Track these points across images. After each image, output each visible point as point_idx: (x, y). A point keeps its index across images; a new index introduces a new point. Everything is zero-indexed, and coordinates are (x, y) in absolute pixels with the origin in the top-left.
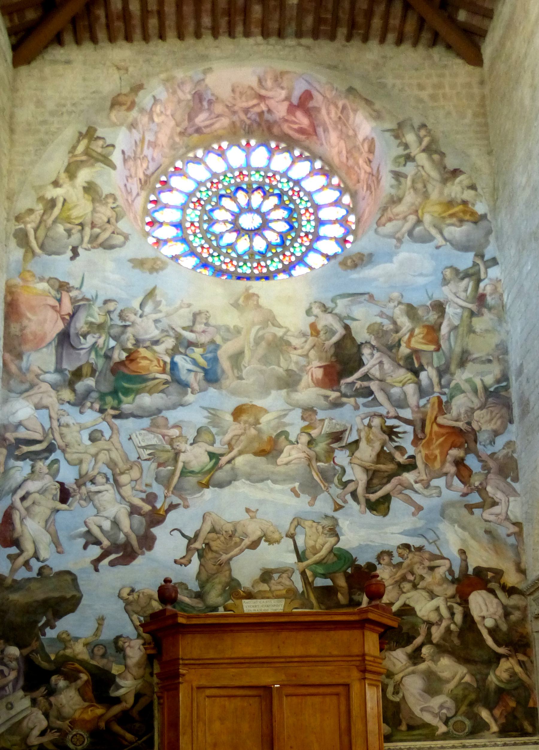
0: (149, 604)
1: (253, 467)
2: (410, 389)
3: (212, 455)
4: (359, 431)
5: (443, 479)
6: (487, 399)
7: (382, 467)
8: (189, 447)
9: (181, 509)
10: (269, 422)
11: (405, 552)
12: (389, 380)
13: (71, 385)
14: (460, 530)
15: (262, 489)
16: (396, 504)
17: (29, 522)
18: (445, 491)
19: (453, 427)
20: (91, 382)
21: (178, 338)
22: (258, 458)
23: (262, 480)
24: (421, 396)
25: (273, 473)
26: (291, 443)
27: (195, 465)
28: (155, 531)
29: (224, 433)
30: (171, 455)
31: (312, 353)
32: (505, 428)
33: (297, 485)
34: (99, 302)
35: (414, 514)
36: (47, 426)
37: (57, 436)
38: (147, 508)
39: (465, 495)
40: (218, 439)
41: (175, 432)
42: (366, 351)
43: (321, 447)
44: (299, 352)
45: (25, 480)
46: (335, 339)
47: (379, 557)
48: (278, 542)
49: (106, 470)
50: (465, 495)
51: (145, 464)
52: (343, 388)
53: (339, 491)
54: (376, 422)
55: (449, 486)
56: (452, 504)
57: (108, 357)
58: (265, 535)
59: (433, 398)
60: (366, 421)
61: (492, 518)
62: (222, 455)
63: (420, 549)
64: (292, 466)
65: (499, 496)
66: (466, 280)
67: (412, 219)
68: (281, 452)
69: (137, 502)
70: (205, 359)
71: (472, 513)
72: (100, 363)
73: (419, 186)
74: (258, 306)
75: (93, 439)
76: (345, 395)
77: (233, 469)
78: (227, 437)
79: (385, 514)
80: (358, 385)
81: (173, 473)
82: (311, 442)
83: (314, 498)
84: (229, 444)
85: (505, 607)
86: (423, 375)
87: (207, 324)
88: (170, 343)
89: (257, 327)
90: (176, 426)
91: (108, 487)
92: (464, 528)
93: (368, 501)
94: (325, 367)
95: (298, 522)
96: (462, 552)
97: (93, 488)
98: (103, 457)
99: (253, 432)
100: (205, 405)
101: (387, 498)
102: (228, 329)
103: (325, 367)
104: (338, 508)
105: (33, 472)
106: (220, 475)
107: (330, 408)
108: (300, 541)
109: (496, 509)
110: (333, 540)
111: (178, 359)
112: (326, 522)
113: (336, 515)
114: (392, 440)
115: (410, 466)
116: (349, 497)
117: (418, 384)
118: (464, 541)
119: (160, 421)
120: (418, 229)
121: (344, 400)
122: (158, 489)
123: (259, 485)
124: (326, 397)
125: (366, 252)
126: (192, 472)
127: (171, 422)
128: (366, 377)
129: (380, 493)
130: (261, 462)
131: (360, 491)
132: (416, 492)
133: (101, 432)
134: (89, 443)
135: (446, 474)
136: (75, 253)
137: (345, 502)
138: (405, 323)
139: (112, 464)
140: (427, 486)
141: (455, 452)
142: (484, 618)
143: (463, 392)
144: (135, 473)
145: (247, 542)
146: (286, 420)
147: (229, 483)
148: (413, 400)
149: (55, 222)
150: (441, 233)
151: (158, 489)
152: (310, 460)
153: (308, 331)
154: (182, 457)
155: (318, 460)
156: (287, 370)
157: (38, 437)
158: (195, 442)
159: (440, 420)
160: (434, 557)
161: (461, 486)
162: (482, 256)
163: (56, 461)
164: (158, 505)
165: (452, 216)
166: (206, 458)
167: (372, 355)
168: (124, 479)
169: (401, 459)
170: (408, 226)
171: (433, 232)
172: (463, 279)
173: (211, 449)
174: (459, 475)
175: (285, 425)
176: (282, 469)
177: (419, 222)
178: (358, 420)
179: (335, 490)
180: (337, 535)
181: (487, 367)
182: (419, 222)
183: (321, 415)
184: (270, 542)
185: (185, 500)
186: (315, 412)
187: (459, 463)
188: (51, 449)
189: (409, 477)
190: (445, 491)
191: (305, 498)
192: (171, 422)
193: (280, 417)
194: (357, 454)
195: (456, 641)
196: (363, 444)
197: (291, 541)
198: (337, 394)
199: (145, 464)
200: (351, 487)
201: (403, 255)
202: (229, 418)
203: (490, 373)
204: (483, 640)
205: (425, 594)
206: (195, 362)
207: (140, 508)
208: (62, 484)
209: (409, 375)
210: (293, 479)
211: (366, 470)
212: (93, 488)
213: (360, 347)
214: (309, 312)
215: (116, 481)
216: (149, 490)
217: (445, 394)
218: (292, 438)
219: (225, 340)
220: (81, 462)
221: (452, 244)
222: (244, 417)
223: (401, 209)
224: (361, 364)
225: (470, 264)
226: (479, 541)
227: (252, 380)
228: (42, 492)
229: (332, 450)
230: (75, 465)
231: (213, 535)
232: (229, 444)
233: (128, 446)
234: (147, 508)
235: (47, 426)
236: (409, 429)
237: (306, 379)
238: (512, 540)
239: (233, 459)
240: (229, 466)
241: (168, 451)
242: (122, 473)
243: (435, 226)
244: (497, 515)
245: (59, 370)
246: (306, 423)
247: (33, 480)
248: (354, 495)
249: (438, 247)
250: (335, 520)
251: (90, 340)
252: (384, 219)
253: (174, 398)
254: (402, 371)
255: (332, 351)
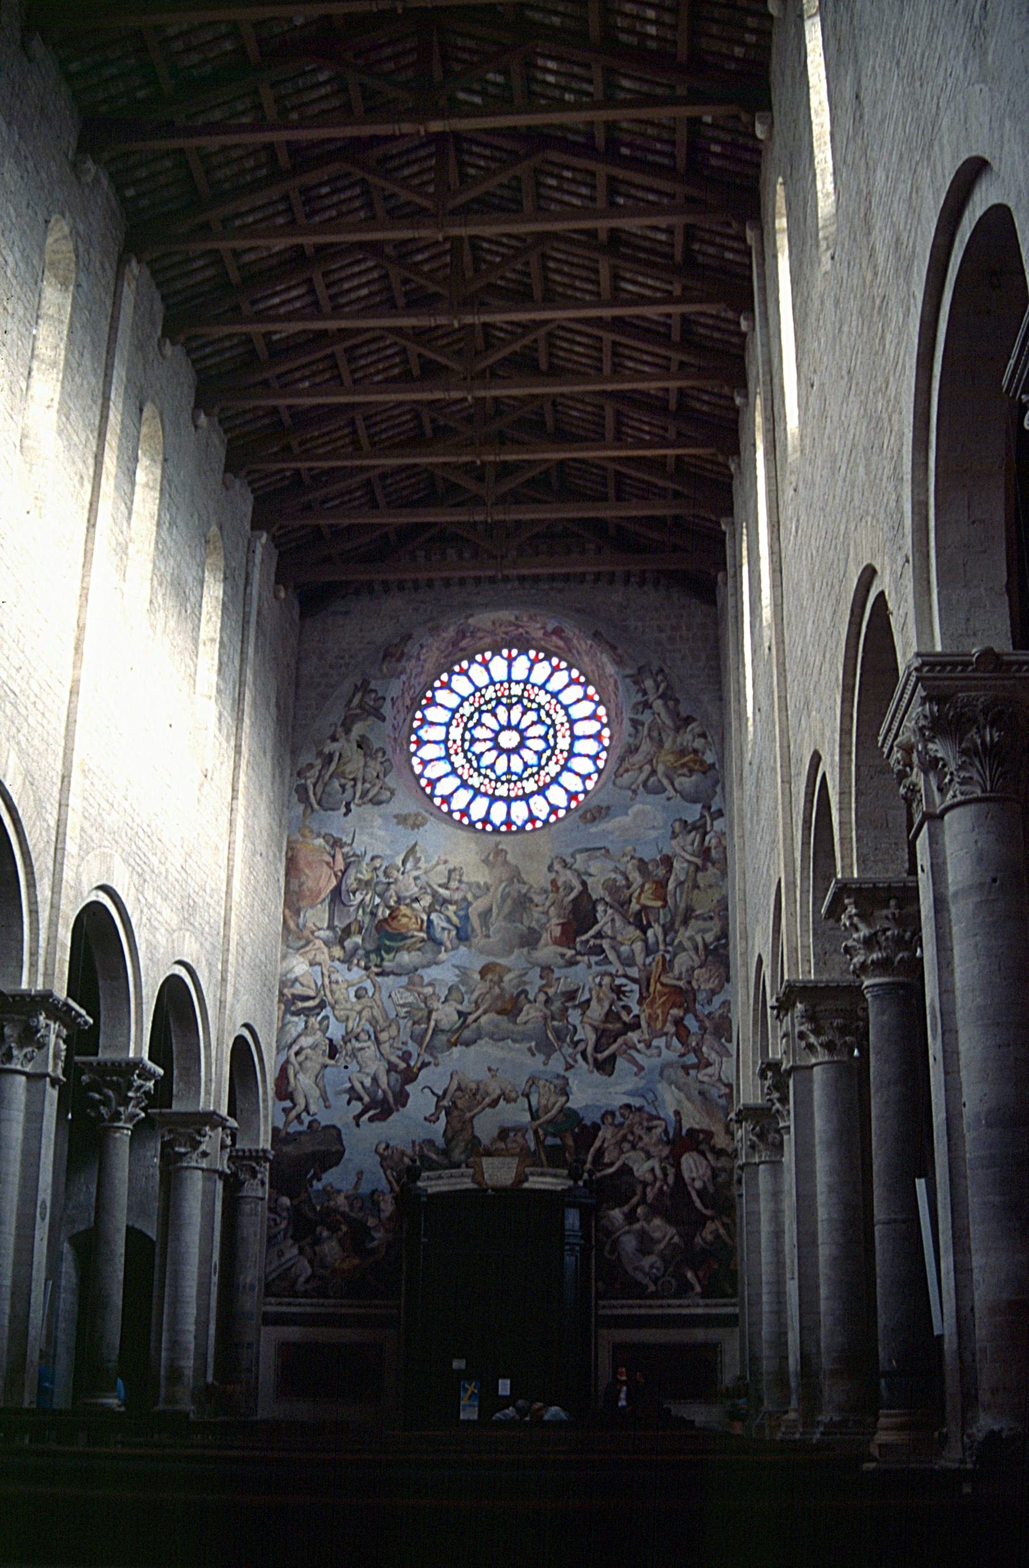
0: (401, 1160)
1: (497, 1026)
2: (638, 946)
3: (460, 1014)
4: (590, 990)
5: (664, 1039)
6: (707, 957)
7: (610, 1026)
8: (440, 1006)
9: (432, 1067)
10: (511, 980)
11: (626, 1113)
12: (619, 938)
13: (341, 942)
14: (676, 1091)
15: (502, 1048)
16: (621, 1063)
17: (301, 1076)
18: (664, 1051)
19: (675, 986)
20: (358, 939)
21: (435, 894)
22: (500, 1017)
23: (503, 1039)
24: (647, 955)
25: (513, 1032)
26: (530, 1002)
27: (445, 1025)
28: (408, 1088)
29: (472, 992)
30: (425, 1013)
31: (552, 911)
32: (722, 987)
33: (533, 1044)
34: (368, 858)
35: (636, 1074)
36: (319, 983)
37: (328, 994)
38: (403, 1065)
39: (682, 1055)
40: (466, 997)
41: (429, 990)
42: (600, 908)
43: (556, 1006)
44: (540, 909)
45: (299, 1036)
46: (573, 895)
47: (603, 1117)
48: (515, 1100)
49: (368, 1027)
50: (682, 1055)
51: (401, 1021)
52: (578, 947)
53: (570, 1050)
54: (607, 980)
55: (668, 1047)
56: (669, 1065)
57: (373, 914)
58: (503, 1094)
59: (658, 957)
60: (598, 980)
61: (706, 1079)
62: (470, 1014)
63: (640, 1109)
64: (529, 1026)
65: (713, 1057)
66: (693, 834)
67: (647, 768)
68: (521, 1011)
69: (394, 1059)
70: (458, 916)
71: (688, 1074)
72: (367, 919)
73: (655, 734)
74: (506, 862)
75: (358, 997)
76: (578, 953)
77: (478, 1028)
78: (476, 994)
79: (610, 1075)
80: (591, 943)
81: (427, 1030)
82: (548, 1001)
83: (548, 1057)
84: (476, 1002)
85: (713, 1169)
86: (650, 933)
87: (460, 881)
88: (426, 901)
89: (503, 885)
90: (430, 984)
91: (369, 1043)
92: (679, 1089)
93: (595, 1060)
94: (563, 925)
95: (533, 1081)
96: (677, 1113)
97: (358, 1045)
98: (366, 1014)
99: (497, 990)
100: (458, 963)
101: (613, 1057)
102: (478, 885)
103: (563, 925)
104: (569, 1067)
105: (306, 1027)
106: (467, 1034)
107: (566, 966)
108: (534, 1101)
109: (710, 1070)
110: (563, 1099)
111: (433, 916)
112: (556, 1082)
113: (567, 1074)
114: (620, 999)
115: (635, 1026)
116: (579, 1057)
117: (645, 941)
118: (679, 1102)
119: (417, 979)
120: (652, 779)
121: (579, 958)
122: (412, 1047)
123: (500, 1044)
124: (563, 955)
125: (604, 804)
126: (443, 1031)
127: (426, 980)
128: (599, 935)
129: (606, 1053)
130: (503, 1021)
131: (590, 1050)
132: (638, 1051)
133: (366, 989)
134: (354, 1000)
135: (666, 1034)
136: (348, 810)
137: (576, 1061)
138: (636, 877)
139: (373, 1021)
140: (649, 1046)
141: (675, 1012)
142: (693, 1180)
143: (685, 950)
144: (393, 1031)
145: (488, 1100)
146: (526, 979)
147: (475, 1042)
148: (639, 959)
149: (331, 777)
150: (672, 784)
151: (412, 1047)
152: (545, 1018)
153: (549, 887)
154: (434, 1016)
155: (553, 1019)
156: (529, 928)
157: (312, 993)
158: (446, 1000)
159: (664, 979)
160: (652, 1118)
161: (679, 1045)
162: (709, 808)
163: (326, 1017)
164: (412, 1063)
165: (683, 765)
166: (456, 1017)
167: (606, 911)
168: (384, 1036)
169: (626, 1018)
170: (643, 776)
171: (665, 782)
172: (690, 832)
173: (460, 1007)
174: (677, 1034)
175: (525, 983)
176: (521, 1028)
177: (654, 772)
178: (590, 978)
179: (568, 1050)
180: (567, 1095)
181: (709, 924)
182: (654, 772)
183: (557, 973)
184: (508, 1101)
185: (436, 1058)
186: (553, 971)
187: (678, 1022)
188: (322, 1005)
189: (633, 1036)
190: (664, 1051)
191: (540, 1057)
192: (426, 980)
193: (521, 976)
194: (588, 1013)
195: (668, 1202)
196: (594, 1003)
197: (526, 1100)
198: (573, 952)
199: (401, 1021)
200: (581, 1047)
201: (637, 807)
202: (477, 977)
203: (711, 930)
204: (693, 1203)
205: (643, 1155)
206: (449, 920)
207: (396, 1066)
208: (331, 1041)
209: (638, 933)
210: (530, 1039)
211: (595, 1029)
212: (358, 1045)
213: (595, 903)
214: (550, 868)
215: (376, 1038)
216: (404, 1048)
217: (668, 952)
218: (531, 997)
219: (476, 897)
220: (347, 1019)
221: (682, 797)
222: (489, 976)
223: (638, 758)
224: (596, 922)
225: (698, 816)
226: (693, 1102)
227: (498, 937)
228: (314, 1047)
229: (566, 1009)
230: (342, 1022)
231: (459, 1093)
232: (476, 1002)
233: (388, 1005)
234: (403, 1065)
235: (319, 983)
236: (636, 987)
237: (546, 937)
238: (723, 1102)
239: (479, 1017)
240: (474, 1025)
241: (421, 1009)
242: (382, 1031)
243: (668, 777)
244: (710, 1076)
245: (331, 927)
246: (544, 982)
247: (306, 1035)
248: (584, 1054)
249: (669, 799)
250: (567, 1080)
251: (359, 897)
252: (621, 770)
253: (429, 956)
254: (631, 928)
255: (570, 907)
